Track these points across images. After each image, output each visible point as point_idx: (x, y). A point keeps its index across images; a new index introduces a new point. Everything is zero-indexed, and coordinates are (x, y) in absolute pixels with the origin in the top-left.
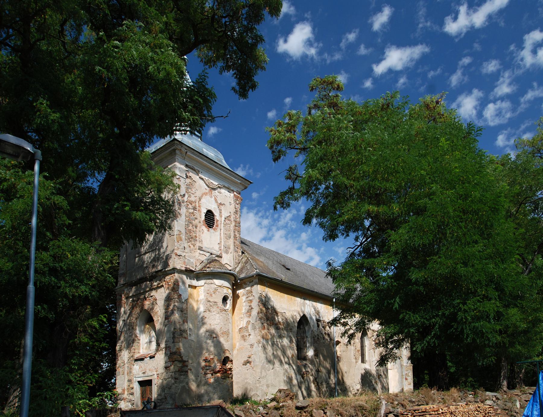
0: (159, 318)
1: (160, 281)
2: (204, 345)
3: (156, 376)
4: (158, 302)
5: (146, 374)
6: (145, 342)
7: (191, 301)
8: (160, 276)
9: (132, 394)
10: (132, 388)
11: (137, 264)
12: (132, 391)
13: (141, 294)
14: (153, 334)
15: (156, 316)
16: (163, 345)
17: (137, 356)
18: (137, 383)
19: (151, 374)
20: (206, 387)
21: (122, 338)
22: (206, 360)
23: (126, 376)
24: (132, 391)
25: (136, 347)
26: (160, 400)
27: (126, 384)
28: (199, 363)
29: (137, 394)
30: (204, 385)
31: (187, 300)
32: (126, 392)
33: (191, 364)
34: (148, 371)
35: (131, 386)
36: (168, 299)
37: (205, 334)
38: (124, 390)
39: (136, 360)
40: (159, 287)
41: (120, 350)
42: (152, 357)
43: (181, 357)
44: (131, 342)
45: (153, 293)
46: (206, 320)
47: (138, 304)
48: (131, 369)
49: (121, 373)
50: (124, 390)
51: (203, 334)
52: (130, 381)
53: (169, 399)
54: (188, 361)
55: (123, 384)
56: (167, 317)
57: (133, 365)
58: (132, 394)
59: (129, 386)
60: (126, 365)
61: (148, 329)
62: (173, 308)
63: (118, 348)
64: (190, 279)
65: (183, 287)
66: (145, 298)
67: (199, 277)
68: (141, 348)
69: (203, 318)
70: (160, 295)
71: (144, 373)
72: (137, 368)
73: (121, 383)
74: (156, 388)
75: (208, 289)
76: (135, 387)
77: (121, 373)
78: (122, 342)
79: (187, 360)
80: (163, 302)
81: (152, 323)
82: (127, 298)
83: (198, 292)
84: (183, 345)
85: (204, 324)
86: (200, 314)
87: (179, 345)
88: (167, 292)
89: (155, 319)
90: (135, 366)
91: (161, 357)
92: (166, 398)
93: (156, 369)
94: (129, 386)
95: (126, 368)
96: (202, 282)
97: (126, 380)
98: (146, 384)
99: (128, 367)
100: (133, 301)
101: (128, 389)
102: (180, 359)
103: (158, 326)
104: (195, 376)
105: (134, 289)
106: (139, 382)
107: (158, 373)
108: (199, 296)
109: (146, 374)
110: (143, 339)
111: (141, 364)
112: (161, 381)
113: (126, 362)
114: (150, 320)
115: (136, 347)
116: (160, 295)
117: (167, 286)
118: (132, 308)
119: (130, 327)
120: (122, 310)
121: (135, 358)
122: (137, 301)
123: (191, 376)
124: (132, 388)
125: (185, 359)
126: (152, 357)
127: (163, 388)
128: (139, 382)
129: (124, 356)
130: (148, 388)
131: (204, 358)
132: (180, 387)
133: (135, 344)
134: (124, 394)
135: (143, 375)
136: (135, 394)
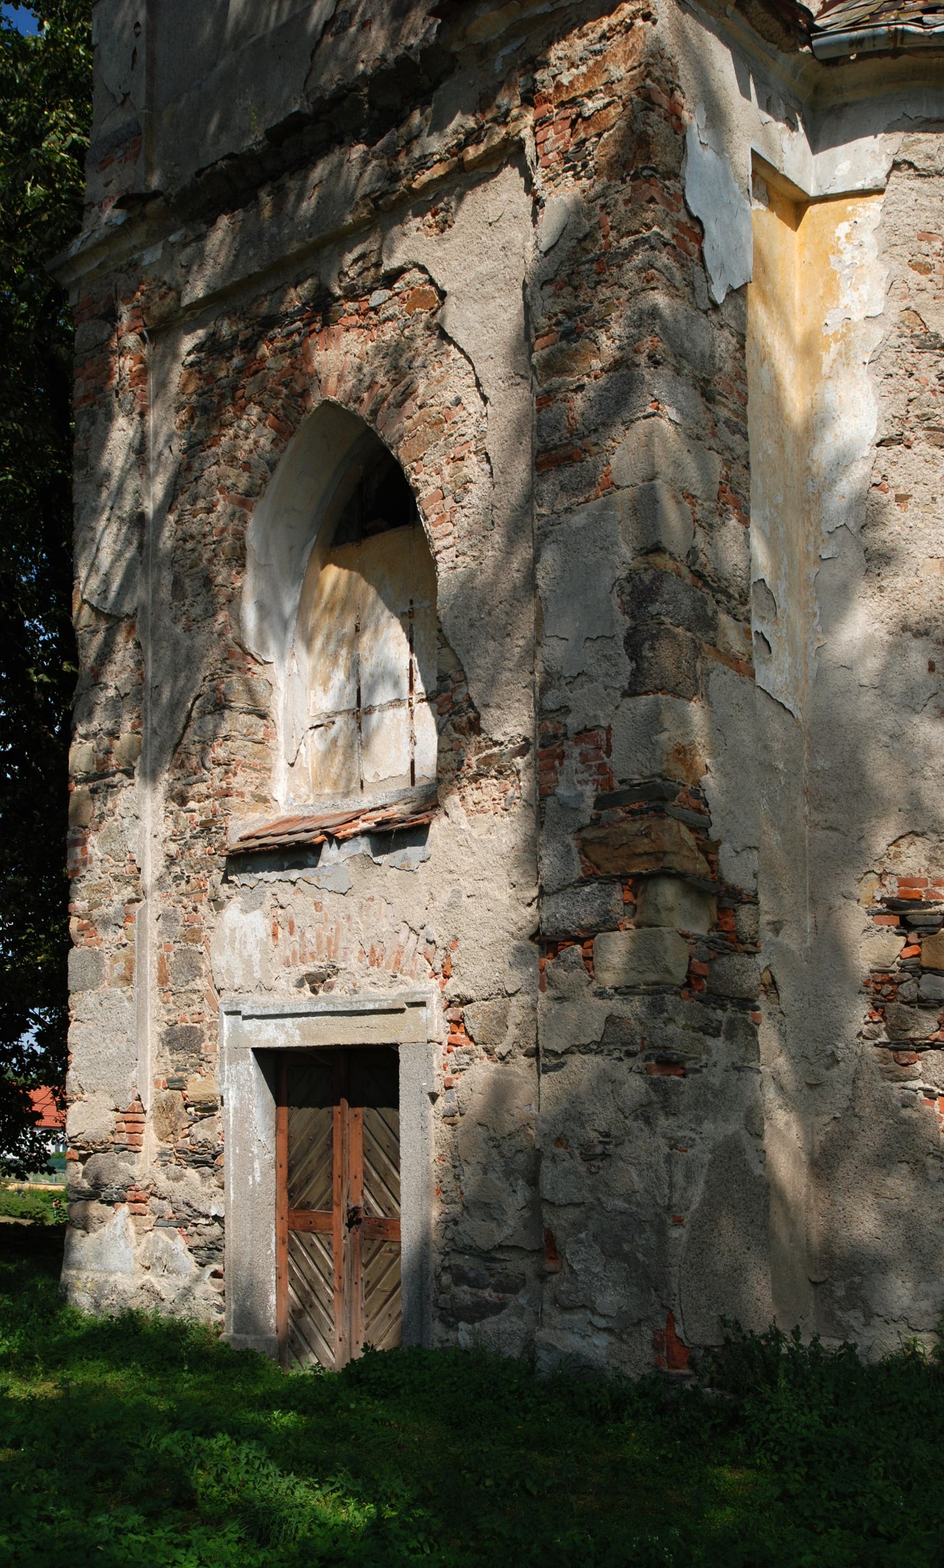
0: (473, 468)
1: (483, 103)
2: (882, 772)
3: (435, 1019)
4: (459, 319)
5: (338, 995)
6: (319, 703)
7: (759, 314)
8: (484, 52)
9: (206, 1159)
10: (208, 1109)
11: (242, 33)
12: (201, 1132)
13: (283, 271)
14: (392, 646)
15: (434, 456)
16: (511, 723)
17: (244, 824)
18: (250, 1068)
19: (388, 995)
20: (900, 1185)
21: (118, 676)
22: (903, 912)
23: (153, 999)
24: (201, 1132)
25: (240, 748)
26: (486, 1256)
27: (150, 1069)
28: (831, 947)
29: (245, 1167)
30: (883, 1161)
31: (737, 294)
32: (150, 1140)
33: (780, 943)
34: (352, 962)
35: (197, 1087)
36: (568, 283)
37: (896, 649)
38: (131, 1117)
39: (247, 859)
40: (466, 176)
41: (100, 778)
42: (392, 836)
43: (709, 848)
44: (189, 723)
45: (413, 242)
46: (898, 524)
47: (252, 367)
48: (193, 935)
49: (112, 969)
50: (131, 1117)
51: (873, 664)
52: (183, 1040)
53: (582, 1257)
54: (753, 900)
55: (131, 1061)
56: (557, 450)
57: (217, 904)
58: (206, 1159)
59: (176, 1085)
60: (154, 905)
61: (346, 603)
62: (631, 345)
63: (80, 755)
64: (767, 105)
65: (709, 155)
66: (322, 310)
67: (837, 111)
68: (281, 764)
69: (867, 513)
70: (480, 256)
71: (315, 981)
72: (246, 928)
73: (112, 1055)
74: (437, 1128)
75: (922, 221)
76: (231, 1102)
77: (112, 969)
78: (115, 706)
79: (746, 883)
80: (507, 312)
81: (385, 543)
82: (161, 331)
83: (826, 251)
84: (719, 729)
85: (879, 561)
86: (842, 463)
87: (684, 722)
88: (563, 194)
89: (428, 479)
90: (232, 913)
91: (483, 832)
92: (549, 1248)
93: (433, 940)
94: (176, 1085)
95: (153, 931)
96: (863, 157)
97: (153, 1031)
98: (334, 1084)
99: (164, 917)
100: (212, 348)
101: (165, 1108)
102: (701, 867)
103: (459, 531)
104: (800, 1059)
105: (220, 236)
106: (269, 1059)
107: (455, 987)
108: (831, 288)
109: (338, 995)
110: (297, 686)
111: (286, 894)
112: (482, 1070)
113: (148, 878)
114: (366, 504)
115: (240, 748)
116: (480, 256)
117: (556, 138)
118: (207, 413)
119: (189, 583)
120: (122, 432)
121: (233, 842)
122: (250, 346)
123: (774, 1055)
124: (208, 1109)
125: (736, 870)
126: (392, 836)
127: (498, 1150)
128: (269, 1059)
129: (132, 831)
130: (351, 1122)
131: (892, 889)
132: (701, 1153)
133: (236, 722)
134: (131, 1148)
135: (304, 999)
136: (229, 1160)
